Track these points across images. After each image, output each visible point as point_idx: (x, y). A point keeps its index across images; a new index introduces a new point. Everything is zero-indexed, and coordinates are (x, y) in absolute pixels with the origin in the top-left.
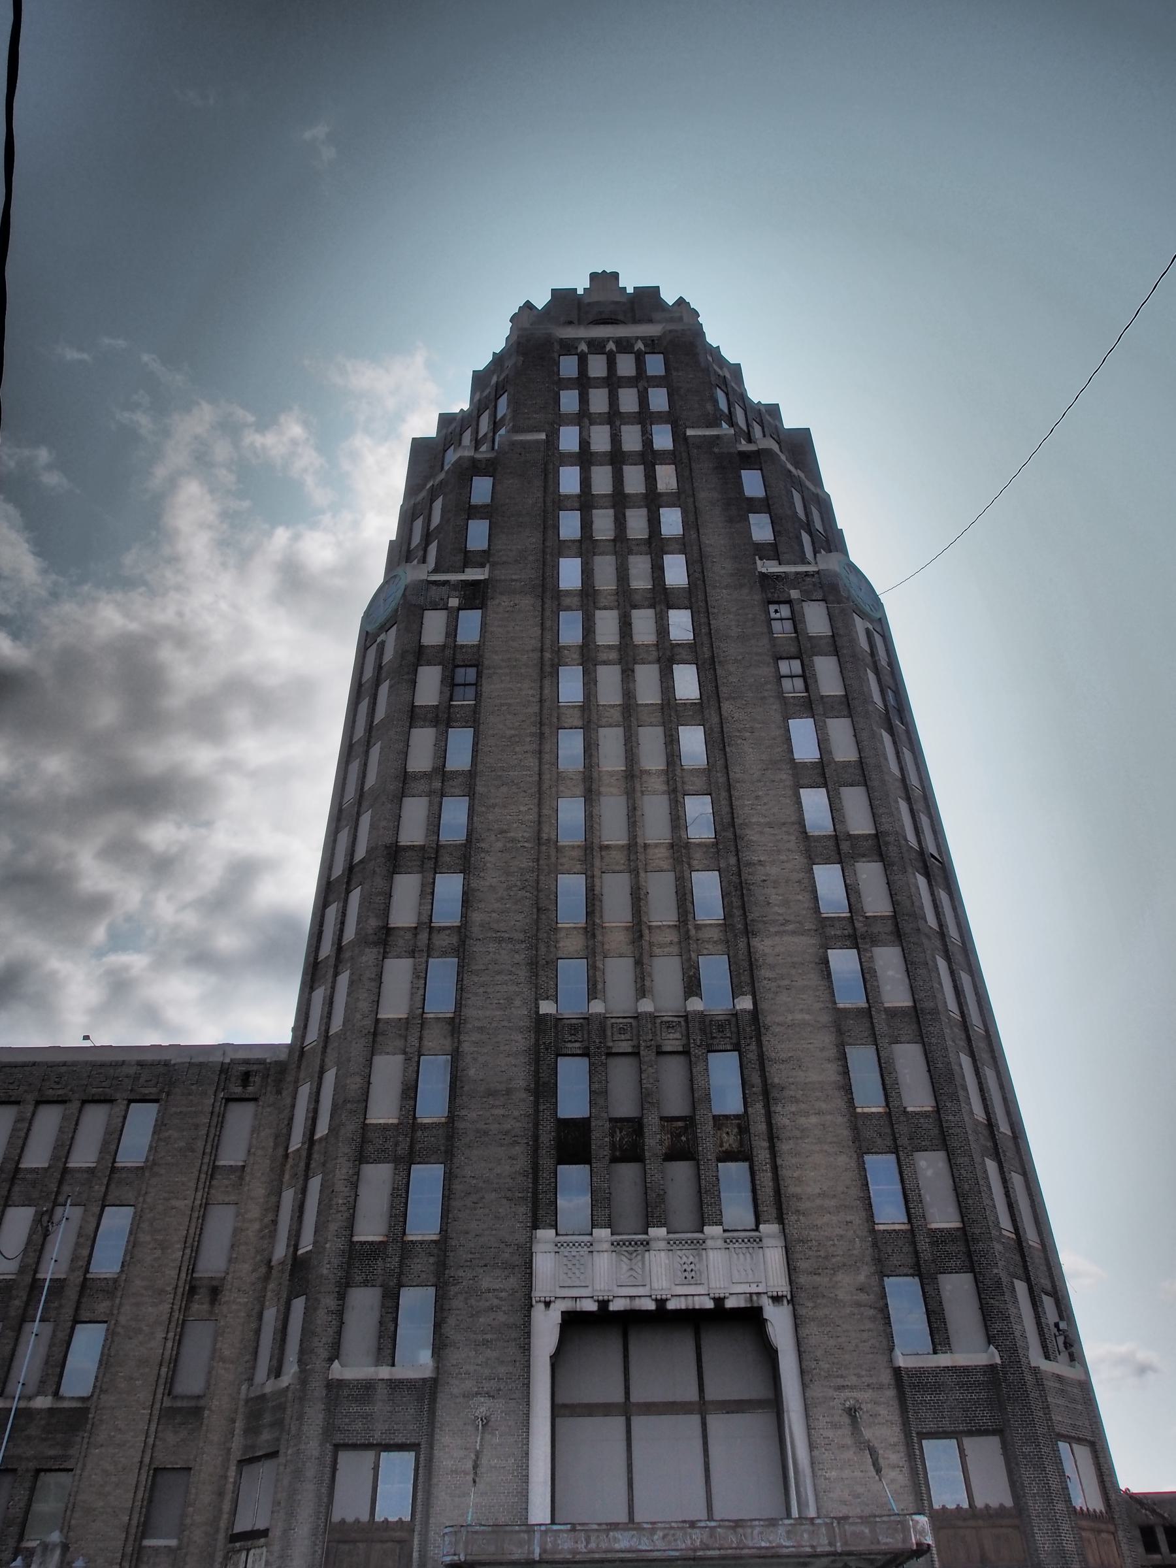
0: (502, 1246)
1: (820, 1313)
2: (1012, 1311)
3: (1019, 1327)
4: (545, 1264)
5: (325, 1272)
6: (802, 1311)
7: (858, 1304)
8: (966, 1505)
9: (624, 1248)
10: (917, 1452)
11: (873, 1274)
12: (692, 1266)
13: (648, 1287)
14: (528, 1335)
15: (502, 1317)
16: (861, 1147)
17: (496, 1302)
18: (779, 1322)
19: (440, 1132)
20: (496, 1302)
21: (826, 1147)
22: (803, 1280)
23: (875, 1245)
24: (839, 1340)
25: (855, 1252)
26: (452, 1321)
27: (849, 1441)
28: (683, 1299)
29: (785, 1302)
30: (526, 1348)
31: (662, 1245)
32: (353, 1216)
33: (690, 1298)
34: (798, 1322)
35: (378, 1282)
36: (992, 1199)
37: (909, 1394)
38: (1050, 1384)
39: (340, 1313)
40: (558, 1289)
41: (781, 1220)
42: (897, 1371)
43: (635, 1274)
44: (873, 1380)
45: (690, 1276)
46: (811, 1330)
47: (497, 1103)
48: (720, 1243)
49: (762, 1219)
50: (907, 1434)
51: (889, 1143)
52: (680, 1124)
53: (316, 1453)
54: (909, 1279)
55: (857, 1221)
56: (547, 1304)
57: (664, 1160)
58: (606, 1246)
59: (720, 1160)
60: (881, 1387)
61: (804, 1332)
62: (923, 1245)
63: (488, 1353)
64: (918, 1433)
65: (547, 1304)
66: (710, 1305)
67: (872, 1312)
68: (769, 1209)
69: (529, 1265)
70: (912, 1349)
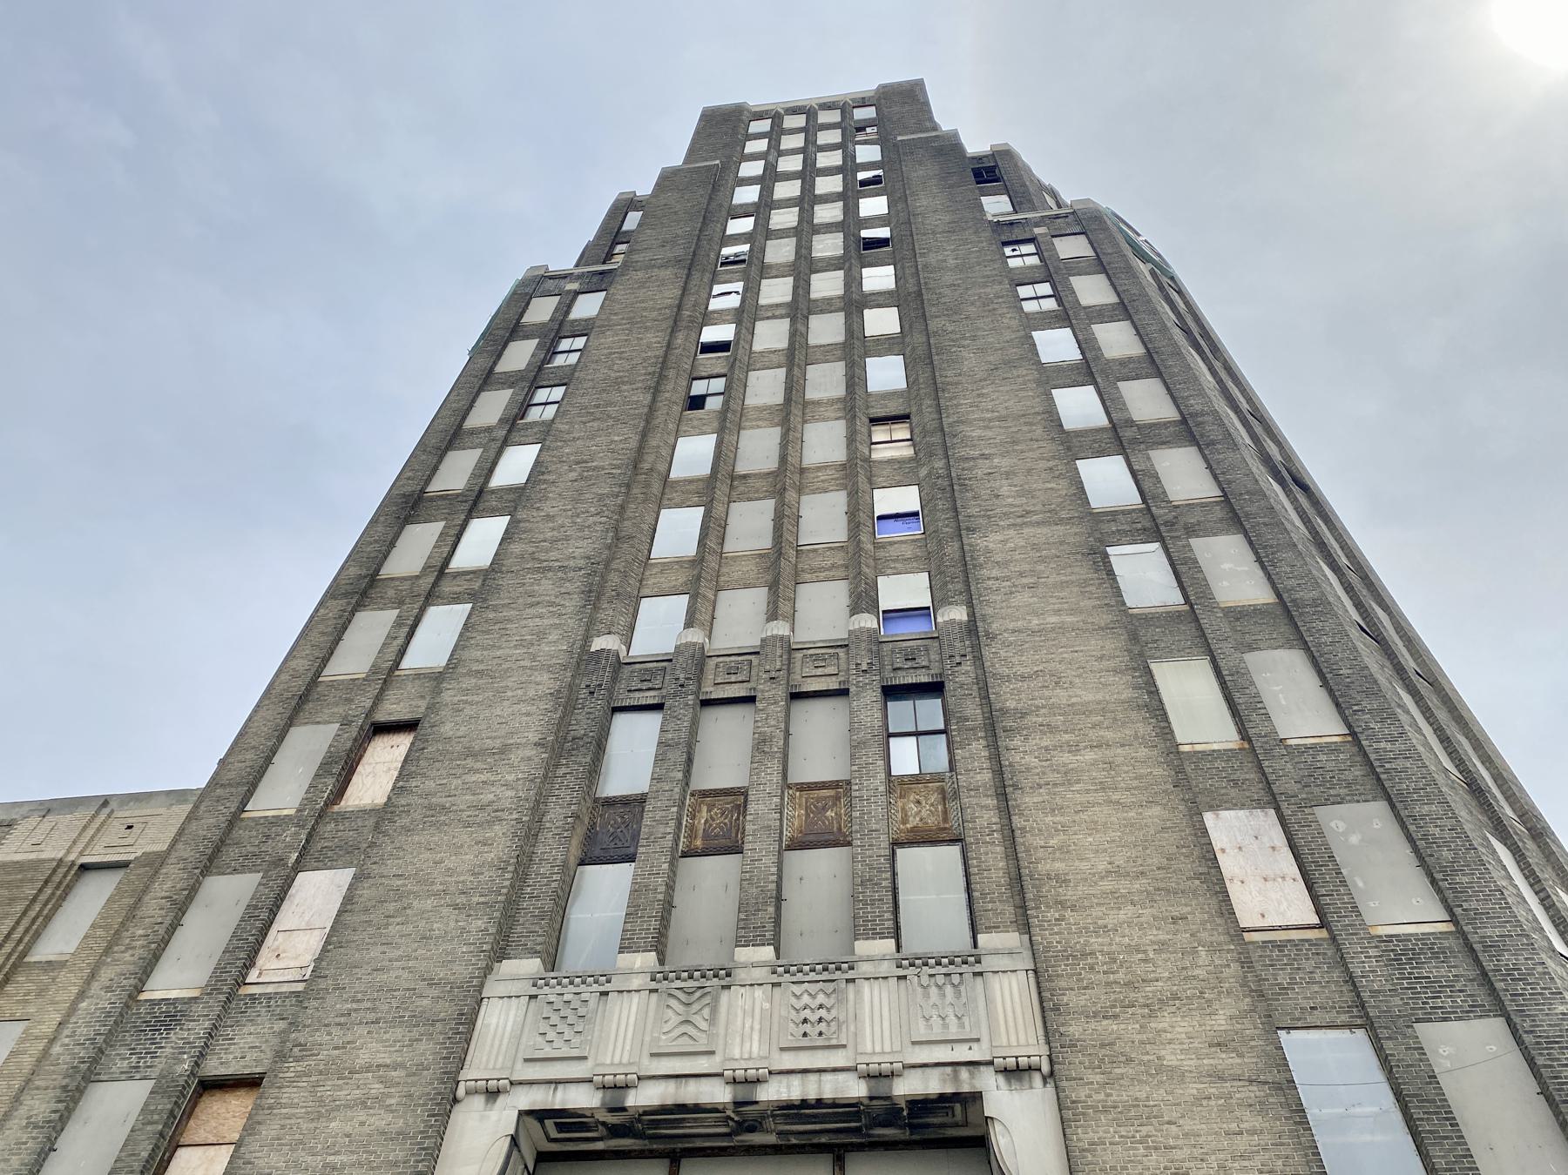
1: (1119, 1096)
7: (1218, 1076)
9: (678, 984)
11: (1243, 1015)
12: (823, 1013)
13: (717, 1058)
17: (377, 1088)
20: (377, 1088)
22: (1074, 1029)
28: (796, 1080)
29: (1037, 1079)
31: (760, 974)
33: (813, 1077)
34: (1068, 1114)
35: (155, 1073)
40: (519, 1064)
41: (1025, 926)
45: (816, 1032)
48: (887, 968)
54: (1345, 1034)
56: (492, 1094)
69: (467, 1022)
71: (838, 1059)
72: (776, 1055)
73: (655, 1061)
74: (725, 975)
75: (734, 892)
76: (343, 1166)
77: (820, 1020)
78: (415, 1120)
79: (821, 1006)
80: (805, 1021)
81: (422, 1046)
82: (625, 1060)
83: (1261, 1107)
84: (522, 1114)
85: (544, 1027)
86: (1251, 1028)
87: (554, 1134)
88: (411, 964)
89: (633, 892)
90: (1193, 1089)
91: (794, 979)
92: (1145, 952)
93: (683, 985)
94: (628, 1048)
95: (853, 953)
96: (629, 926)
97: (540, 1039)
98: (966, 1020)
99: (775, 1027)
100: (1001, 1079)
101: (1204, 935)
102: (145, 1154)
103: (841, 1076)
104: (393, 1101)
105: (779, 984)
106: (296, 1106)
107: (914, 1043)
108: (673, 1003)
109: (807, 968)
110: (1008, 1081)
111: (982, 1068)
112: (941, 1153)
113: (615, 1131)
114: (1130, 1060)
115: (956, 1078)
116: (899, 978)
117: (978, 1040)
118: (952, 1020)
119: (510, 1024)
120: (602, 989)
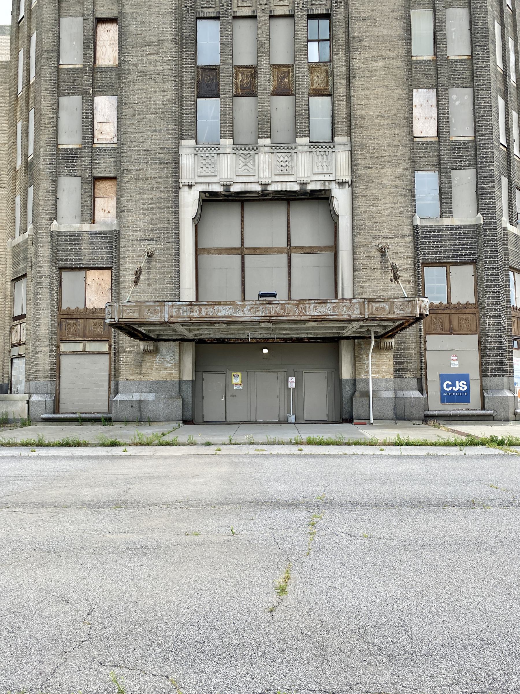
0: (158, 149)
1: (369, 192)
2: (497, 193)
3: (499, 203)
4: (187, 162)
5: (41, 167)
6: (357, 191)
7: (396, 187)
8: (445, 302)
9: (242, 152)
10: (421, 273)
12: (287, 163)
13: (256, 177)
14: (177, 205)
15: (160, 195)
16: (412, 83)
17: (156, 185)
19: (114, 74)
20: (156, 185)
21: (386, 83)
22: (360, 172)
23: (412, 150)
24: (380, 208)
25: (398, 154)
26: (127, 197)
27: (378, 267)
28: (279, 184)
30: (176, 213)
31: (267, 149)
32: (58, 132)
33: (284, 183)
34: (354, 197)
36: (498, 122)
37: (420, 242)
38: (511, 238)
39: (55, 192)
40: (196, 177)
41: (350, 134)
42: (415, 228)
43: (248, 168)
44: (400, 232)
45: (285, 170)
48: (306, 148)
49: (337, 132)
50: (416, 263)
51: (433, 81)
52: (285, 70)
53: (48, 272)
55: (403, 134)
56: (190, 187)
57: (272, 95)
58: (228, 150)
59: (310, 95)
60: (403, 236)
61: (357, 203)
62: (445, 151)
63: (152, 216)
64: (422, 263)
65: (190, 187)
66: (297, 188)
67: (404, 192)
68: (342, 127)
70: (427, 211)
71: (292, 178)
72: (273, 176)
73: (238, 177)
74: (256, 148)
75: (254, 115)
77: (286, 166)
79: (286, 161)
80: (282, 166)
81: (165, 171)
86: (408, 173)
88: (153, 141)
91: (278, 151)
92: (384, 146)
94: (229, 173)
97: (201, 169)
98: (329, 167)
100: (337, 185)
101: (402, 141)
102: (89, 202)
104: (162, 189)
106: (132, 189)
108: (241, 158)
109: (282, 148)
115: (324, 184)
118: (325, 167)
119: (191, 163)
120: (218, 152)
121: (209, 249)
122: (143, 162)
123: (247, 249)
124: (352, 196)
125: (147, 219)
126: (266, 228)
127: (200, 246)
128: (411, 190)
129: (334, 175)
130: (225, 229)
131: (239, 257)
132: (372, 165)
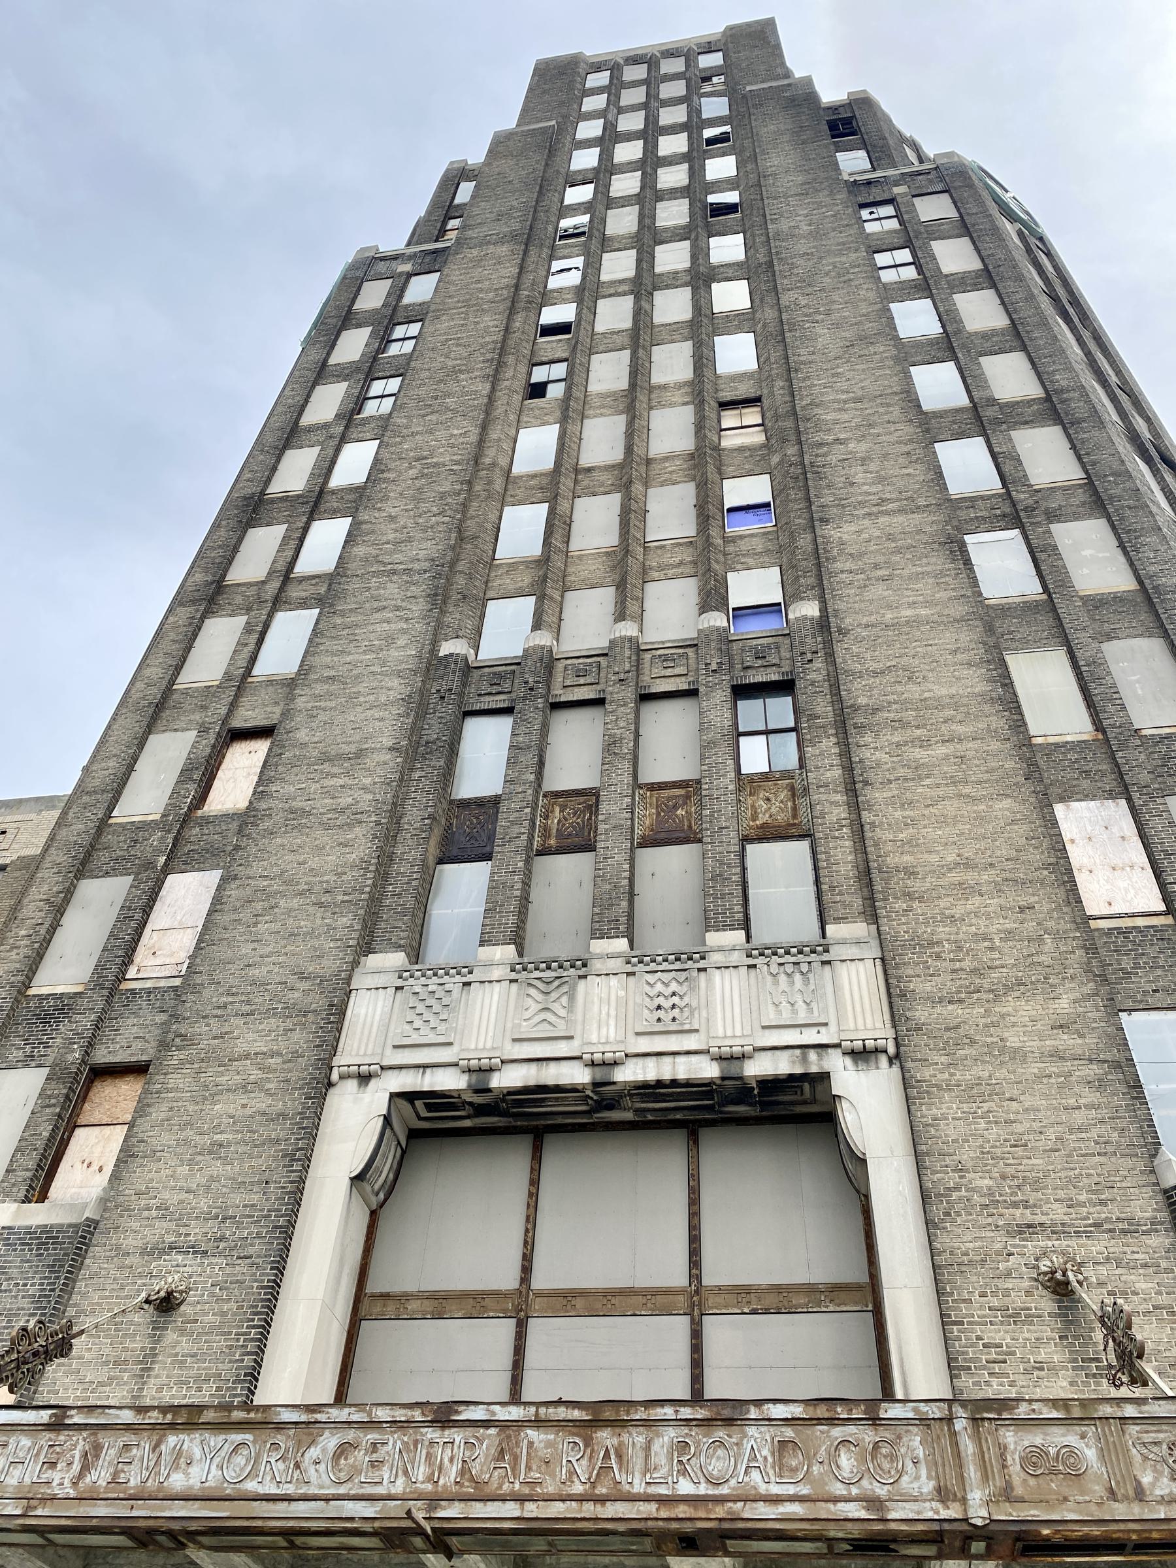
6: (921, 1072)
9: (537, 974)
12: (676, 1000)
13: (576, 1043)
15: (260, 1102)
17: (256, 1074)
18: (868, 1106)
20: (256, 1074)
22: (921, 1014)
28: (651, 1062)
29: (883, 1060)
30: (300, 1160)
31: (616, 964)
34: (913, 1092)
35: (50, 1060)
45: (669, 1019)
46: (940, 1108)
47: (335, 770)
48: (737, 957)
63: (218, 1168)
71: (691, 1043)
74: (581, 965)
75: (588, 886)
76: (229, 1144)
77: (674, 1006)
78: (293, 1103)
79: (674, 994)
80: (659, 1007)
81: (296, 1036)
82: (489, 1045)
83: (1100, 1084)
84: (393, 1096)
85: (410, 1016)
87: (424, 1113)
89: (491, 888)
90: (1034, 1068)
91: (648, 968)
93: (541, 975)
95: (704, 944)
96: (488, 921)
98: (814, 1005)
99: (631, 1014)
100: (848, 1061)
103: (694, 1059)
105: (633, 974)
107: (764, 1027)
108: (532, 991)
109: (660, 959)
110: (855, 1062)
111: (830, 1050)
112: (790, 1128)
113: (480, 1110)
114: (974, 1042)
115: (804, 1060)
116: (749, 967)
117: (826, 1024)
118: (800, 1005)
121: (405, 1297)
122: (237, 1015)
123: (540, 1294)
124: (905, 1089)
125: (200, 1178)
126: (615, 1219)
127: (374, 1286)
128: (1117, 1065)
129: (833, 1027)
130: (470, 1225)
131: (505, 1329)
132: (959, 992)
